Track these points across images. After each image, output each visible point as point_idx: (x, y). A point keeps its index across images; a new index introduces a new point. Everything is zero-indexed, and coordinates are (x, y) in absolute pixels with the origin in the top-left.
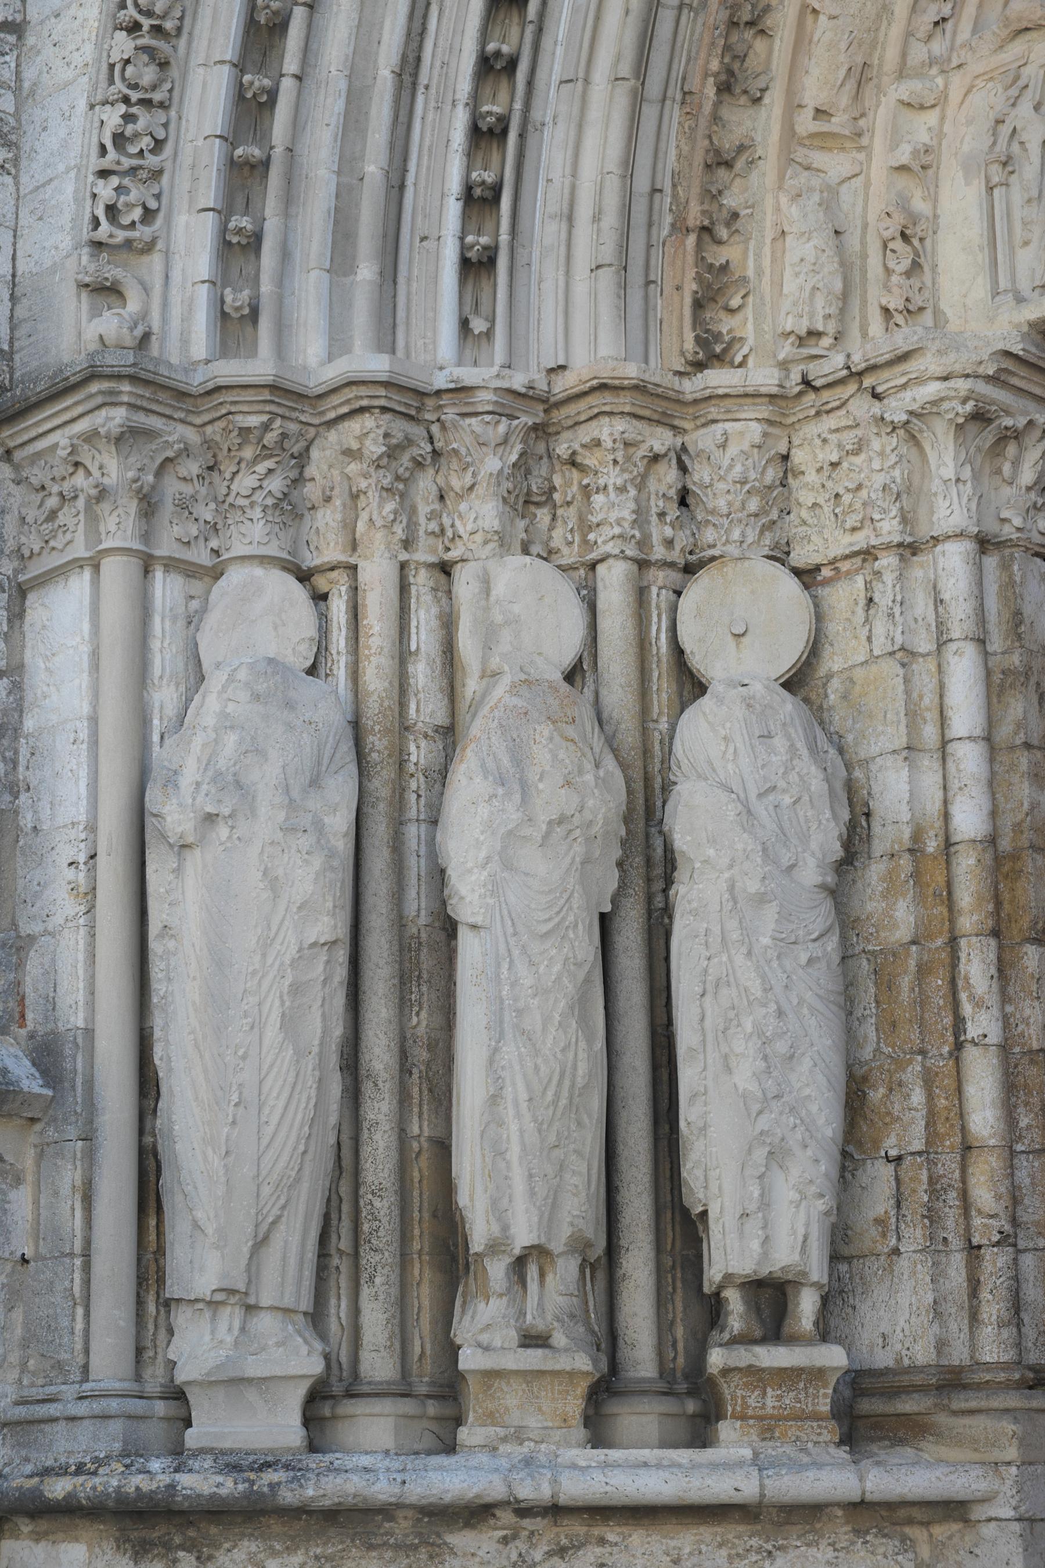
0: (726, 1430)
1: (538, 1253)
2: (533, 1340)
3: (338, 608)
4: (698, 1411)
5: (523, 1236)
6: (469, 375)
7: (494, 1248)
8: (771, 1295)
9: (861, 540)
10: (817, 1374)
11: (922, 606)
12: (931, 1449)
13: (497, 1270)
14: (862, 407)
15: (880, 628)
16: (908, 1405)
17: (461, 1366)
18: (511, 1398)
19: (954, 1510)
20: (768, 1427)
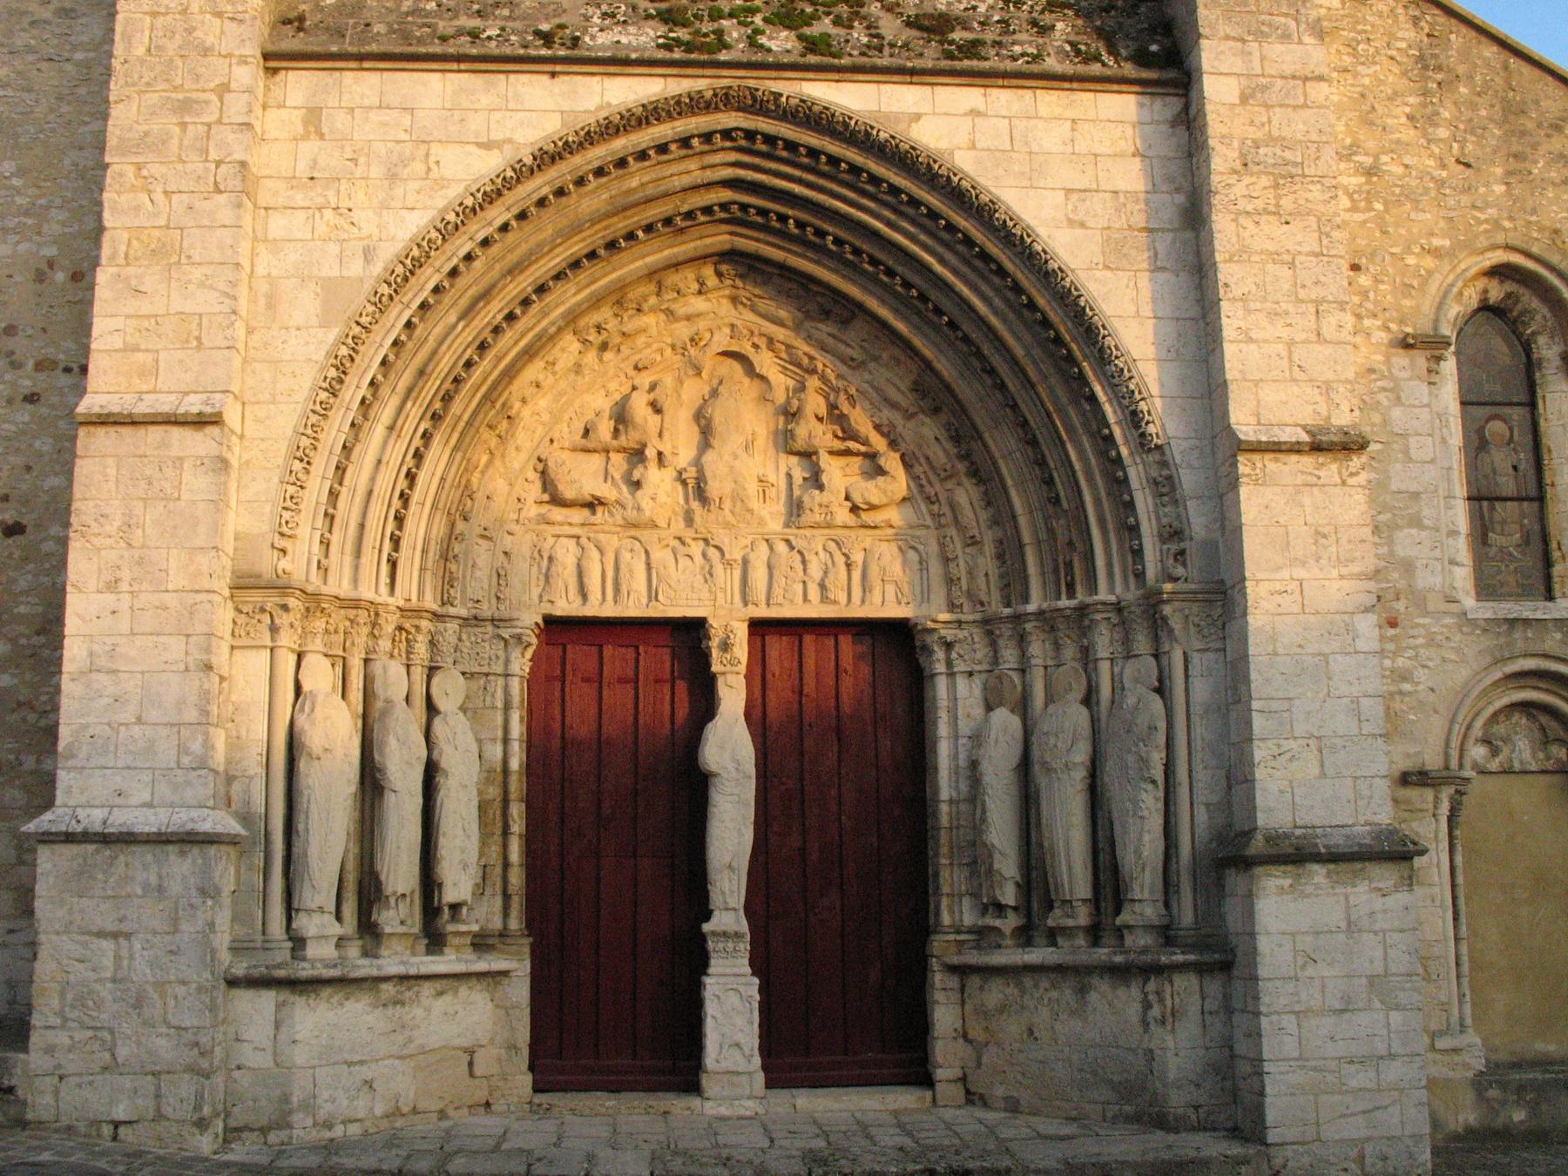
0: (446, 950)
1: (404, 895)
2: (402, 923)
3: (339, 670)
4: (435, 940)
5: (400, 891)
6: (391, 600)
7: (394, 893)
8: (455, 907)
9: (485, 669)
10: (469, 933)
11: (500, 694)
12: (495, 954)
13: (392, 901)
14: (490, 628)
15: (488, 699)
16: (490, 941)
17: (756, 981)
18: (394, 941)
19: (505, 973)
20: (458, 948)
